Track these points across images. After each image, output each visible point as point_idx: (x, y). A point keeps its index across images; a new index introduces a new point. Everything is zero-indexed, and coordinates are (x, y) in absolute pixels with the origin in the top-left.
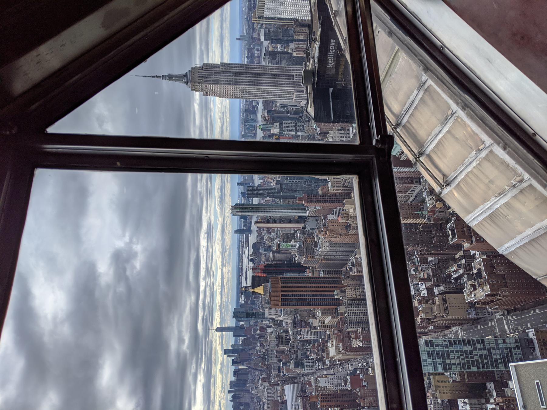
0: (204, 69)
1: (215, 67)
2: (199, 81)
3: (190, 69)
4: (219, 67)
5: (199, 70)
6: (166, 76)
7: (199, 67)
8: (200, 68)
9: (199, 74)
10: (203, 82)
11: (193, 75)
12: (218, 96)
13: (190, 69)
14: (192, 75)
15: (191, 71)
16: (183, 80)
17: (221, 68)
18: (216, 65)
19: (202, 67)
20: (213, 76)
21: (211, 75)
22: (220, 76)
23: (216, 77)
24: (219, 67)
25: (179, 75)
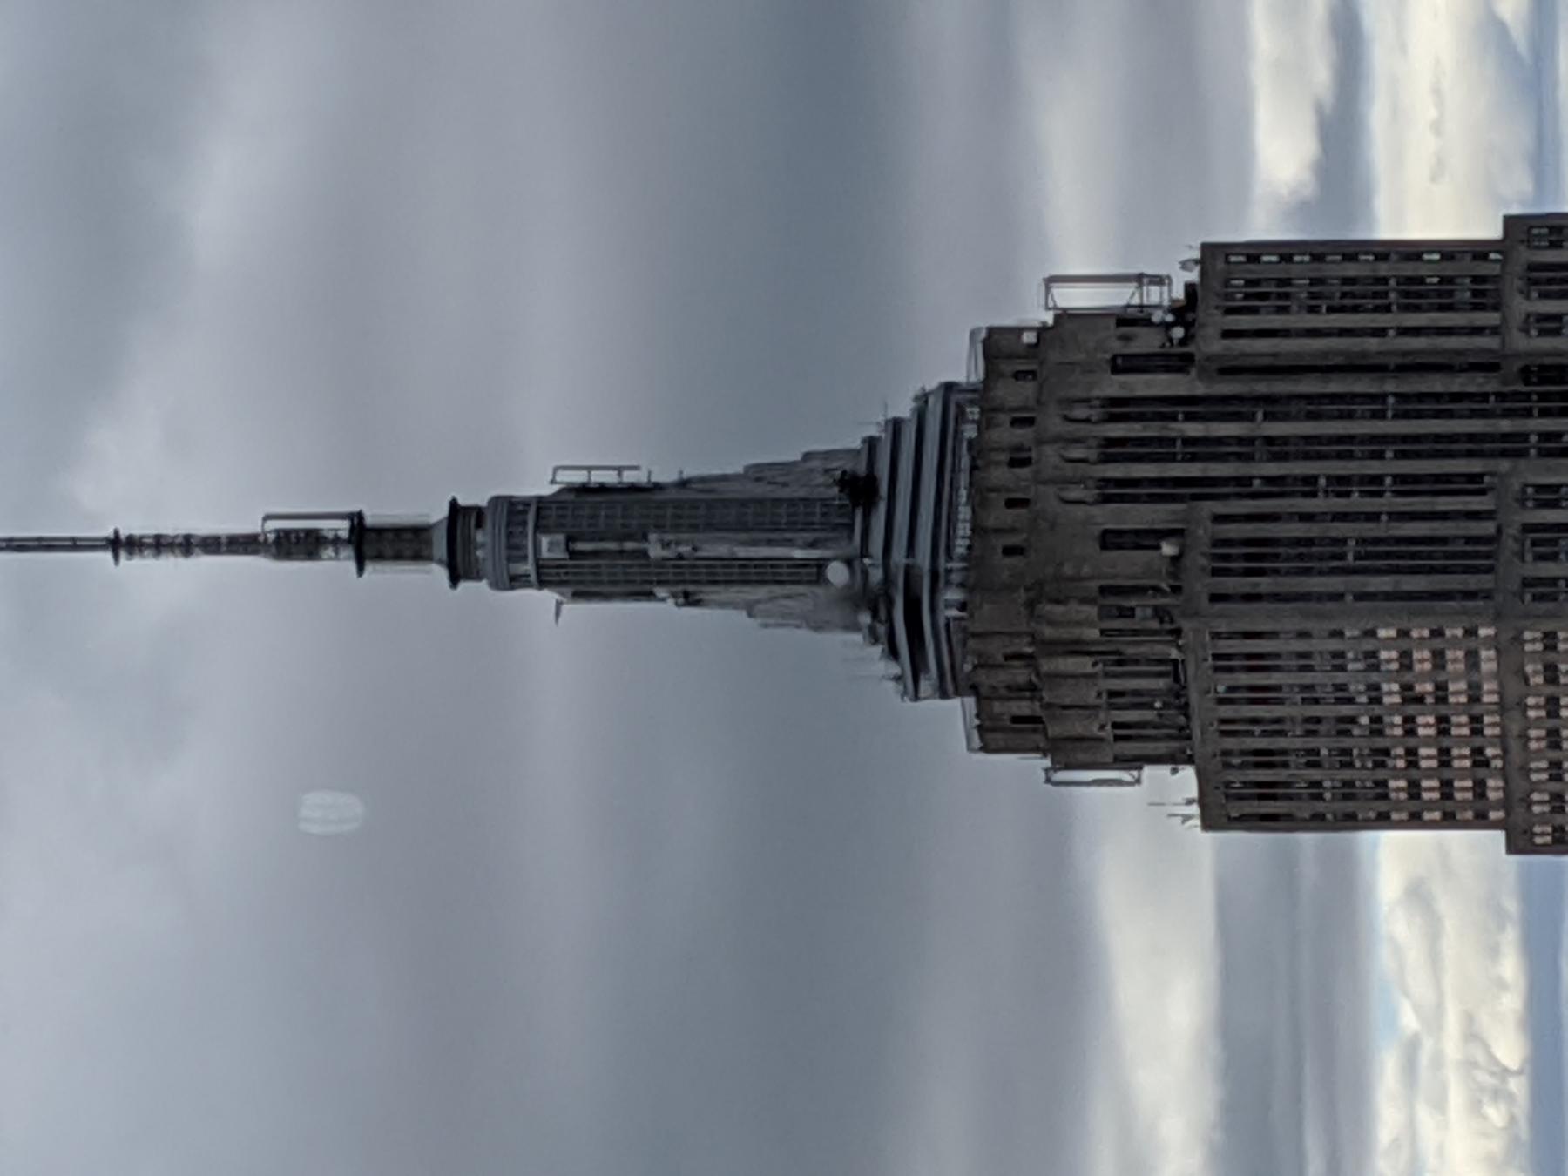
0: (1211, 344)
1: (1414, 293)
2: (1128, 565)
3: (962, 367)
4: (1485, 295)
5: (1124, 365)
6: (512, 509)
7: (1129, 319)
8: (1147, 342)
9: (1112, 450)
10: (1200, 585)
11: (1019, 460)
12: (1481, 821)
13: (962, 367)
14: (1000, 475)
15: (981, 392)
16: (837, 573)
17: (1521, 305)
18: (1430, 269)
19: (1185, 311)
20: (1391, 466)
21: (1343, 447)
22: (1513, 447)
23: (1443, 484)
24: (1485, 295)
25: (757, 473)
